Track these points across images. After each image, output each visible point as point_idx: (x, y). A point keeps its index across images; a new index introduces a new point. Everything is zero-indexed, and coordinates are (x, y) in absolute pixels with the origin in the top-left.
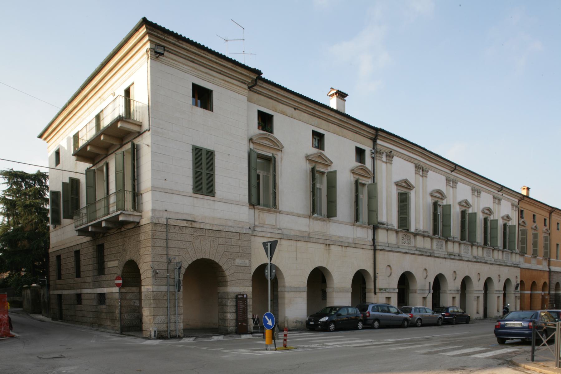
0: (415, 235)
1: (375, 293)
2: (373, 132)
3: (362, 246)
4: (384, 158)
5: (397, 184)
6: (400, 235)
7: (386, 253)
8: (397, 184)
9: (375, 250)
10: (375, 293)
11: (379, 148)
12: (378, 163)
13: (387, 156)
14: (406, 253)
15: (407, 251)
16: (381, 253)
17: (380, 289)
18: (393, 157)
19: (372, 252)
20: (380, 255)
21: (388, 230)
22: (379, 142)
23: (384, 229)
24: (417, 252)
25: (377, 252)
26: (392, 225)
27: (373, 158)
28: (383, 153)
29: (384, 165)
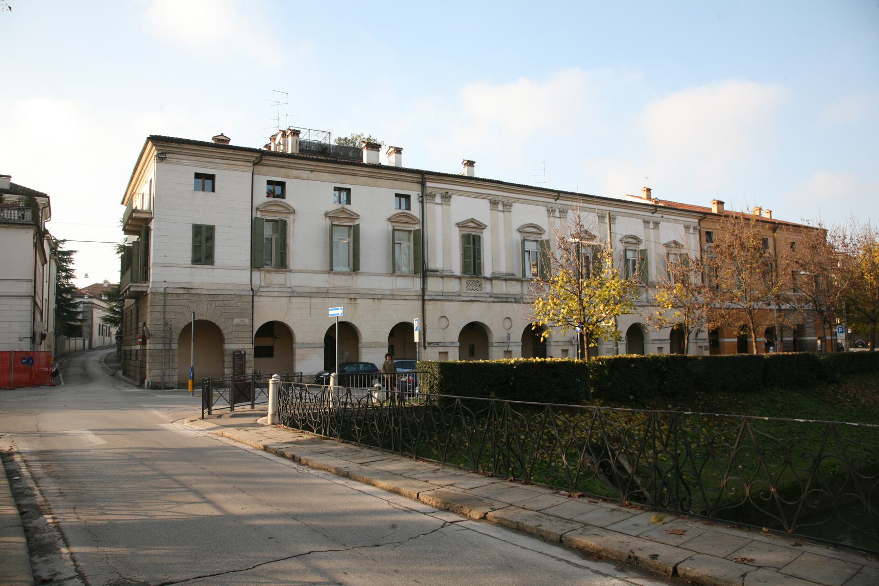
0: (491, 279)
1: (425, 348)
2: (419, 176)
3: (403, 297)
4: (438, 199)
5: (459, 225)
6: (464, 281)
7: (439, 303)
8: (459, 225)
9: (423, 300)
10: (425, 348)
11: (428, 191)
12: (428, 206)
13: (442, 197)
14: (472, 301)
15: (473, 299)
16: (430, 303)
17: (429, 343)
18: (450, 197)
19: (420, 302)
20: (429, 306)
21: (442, 277)
22: (428, 184)
23: (437, 276)
24: (491, 299)
25: (427, 303)
26: (451, 272)
27: (422, 202)
28: (435, 196)
29: (439, 208)
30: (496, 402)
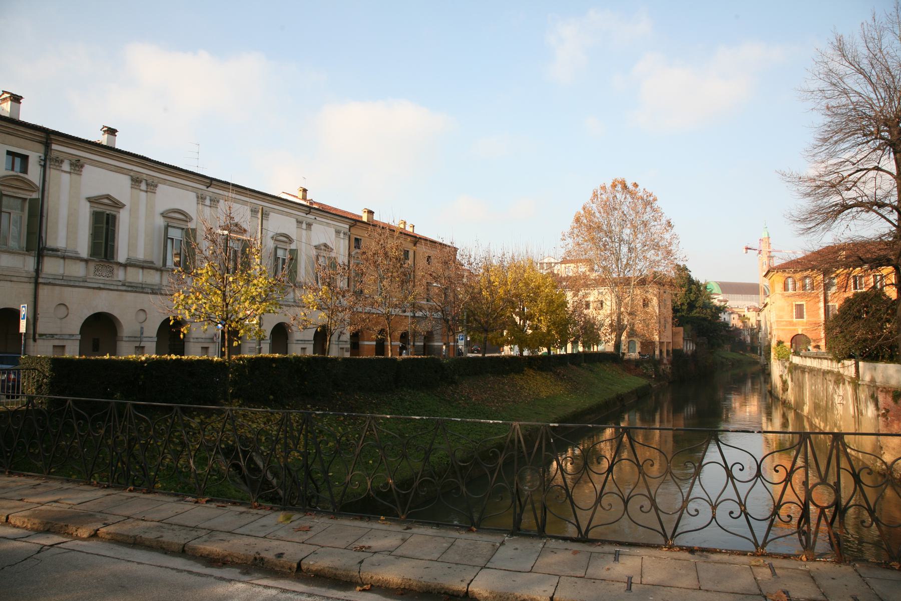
0: (125, 266)
1: (35, 340)
2: (43, 135)
3: (9, 278)
4: (66, 166)
5: (90, 200)
6: (92, 266)
7: (57, 288)
8: (90, 200)
9: (37, 284)
10: (35, 340)
11: (54, 155)
12: (52, 173)
13: (71, 164)
14: (100, 288)
15: (102, 286)
16: (46, 287)
17: (41, 335)
18: (82, 166)
19: (32, 286)
20: (44, 291)
21: (64, 258)
22: (54, 147)
23: (58, 257)
24: (124, 288)
25: (41, 287)
26: (76, 253)
27: (44, 167)
28: (62, 161)
29: (66, 178)
30: (73, 401)
